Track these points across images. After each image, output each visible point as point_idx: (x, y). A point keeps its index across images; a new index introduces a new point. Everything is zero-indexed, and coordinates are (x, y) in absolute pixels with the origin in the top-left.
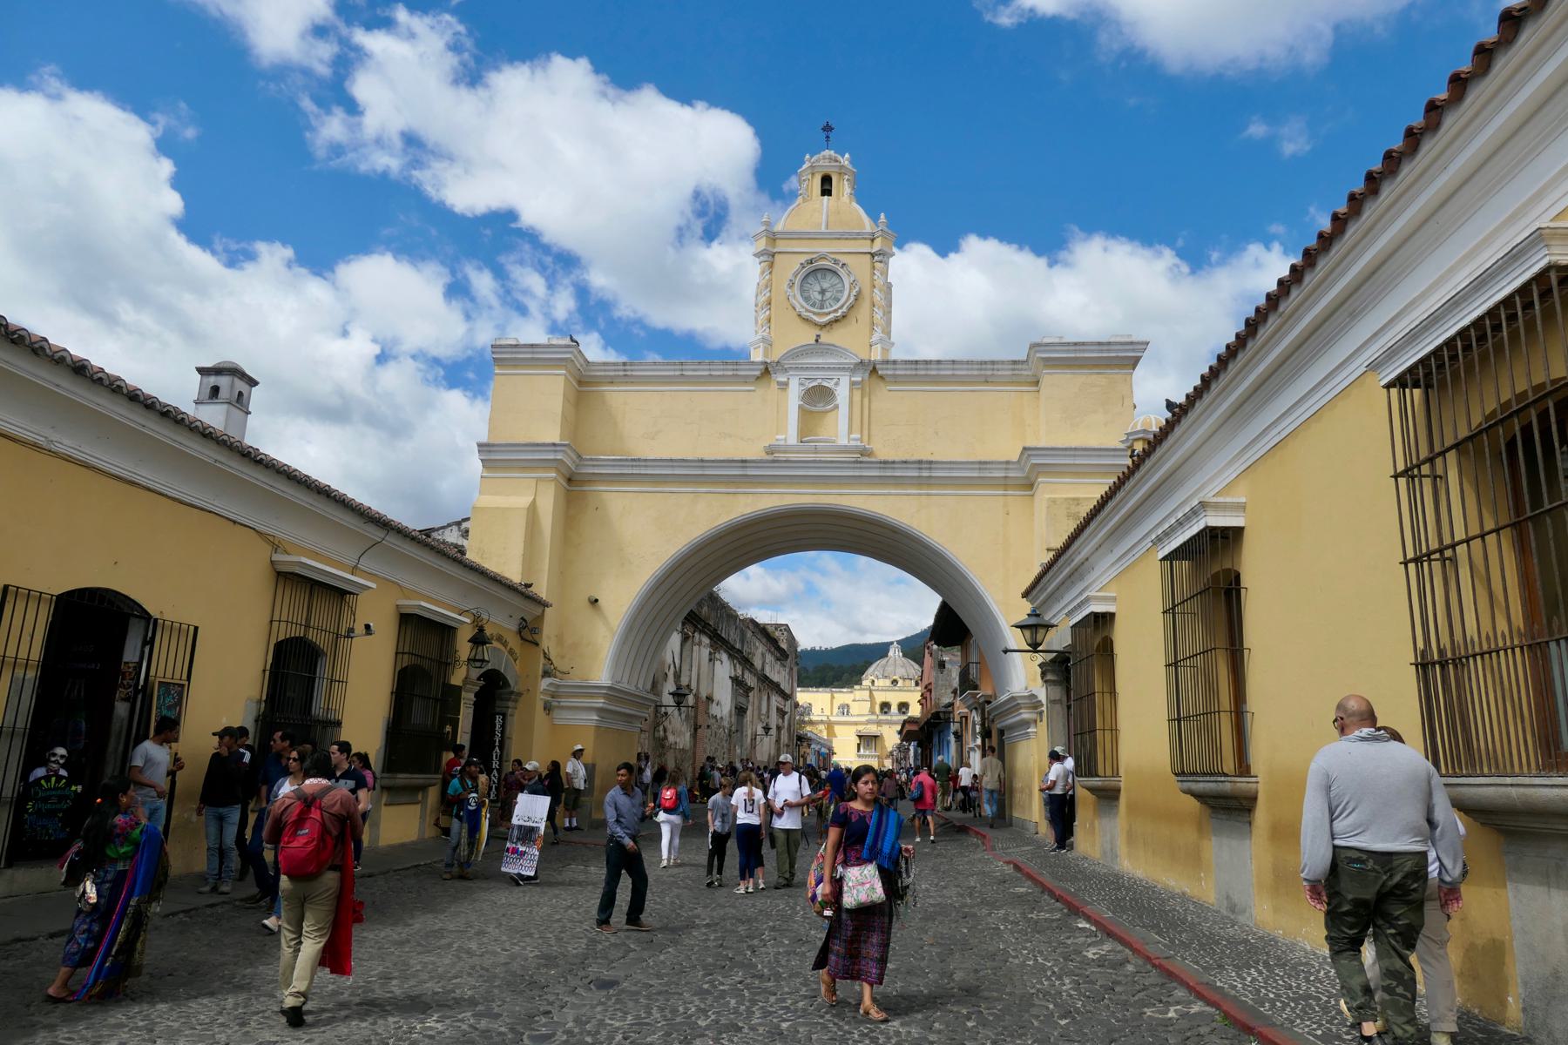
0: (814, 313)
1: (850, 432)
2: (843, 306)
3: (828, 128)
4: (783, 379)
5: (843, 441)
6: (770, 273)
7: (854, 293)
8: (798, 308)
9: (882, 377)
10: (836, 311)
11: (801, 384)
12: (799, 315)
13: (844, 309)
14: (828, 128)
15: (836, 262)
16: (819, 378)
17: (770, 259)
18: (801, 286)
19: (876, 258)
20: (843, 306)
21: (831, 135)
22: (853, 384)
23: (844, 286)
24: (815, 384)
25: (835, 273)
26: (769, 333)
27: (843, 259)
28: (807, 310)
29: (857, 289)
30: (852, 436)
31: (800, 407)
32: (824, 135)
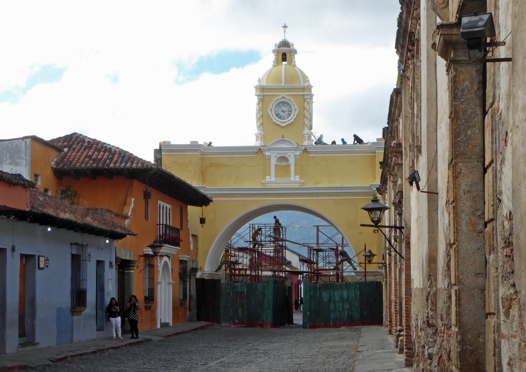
0: (281, 122)
1: (296, 174)
2: (291, 119)
3: (285, 27)
4: (267, 154)
5: (292, 179)
6: (262, 103)
7: (296, 113)
8: (274, 120)
9: (309, 152)
10: (289, 121)
11: (276, 156)
12: (274, 123)
13: (292, 120)
14: (285, 27)
15: (289, 100)
16: (283, 153)
17: (261, 97)
18: (275, 109)
19: (306, 97)
20: (291, 119)
21: (286, 29)
22: (295, 156)
23: (292, 109)
24: (280, 155)
26: (263, 130)
28: (277, 121)
29: (297, 112)
30: (296, 176)
31: (276, 165)
32: (283, 29)
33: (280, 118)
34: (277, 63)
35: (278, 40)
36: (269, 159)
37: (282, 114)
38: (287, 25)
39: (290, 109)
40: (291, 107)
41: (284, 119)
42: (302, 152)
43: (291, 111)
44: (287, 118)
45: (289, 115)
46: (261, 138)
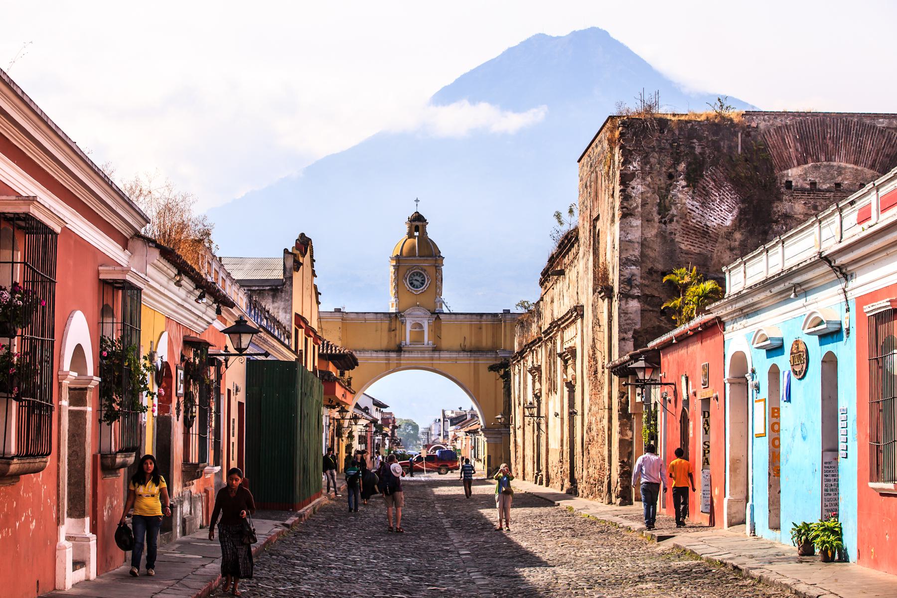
3: (417, 201)
16: (418, 320)
25: (421, 274)
27: (425, 268)
33: (414, 286)
34: (410, 235)
35: (410, 213)
36: (405, 325)
37: (415, 283)
38: (419, 199)
39: (423, 279)
40: (424, 277)
41: (417, 288)
42: (434, 319)
43: (424, 280)
44: (421, 287)
45: (423, 284)
46: (396, 304)
